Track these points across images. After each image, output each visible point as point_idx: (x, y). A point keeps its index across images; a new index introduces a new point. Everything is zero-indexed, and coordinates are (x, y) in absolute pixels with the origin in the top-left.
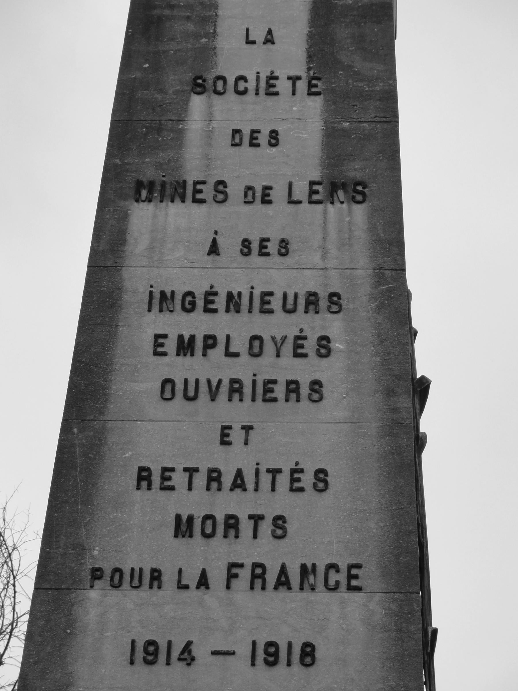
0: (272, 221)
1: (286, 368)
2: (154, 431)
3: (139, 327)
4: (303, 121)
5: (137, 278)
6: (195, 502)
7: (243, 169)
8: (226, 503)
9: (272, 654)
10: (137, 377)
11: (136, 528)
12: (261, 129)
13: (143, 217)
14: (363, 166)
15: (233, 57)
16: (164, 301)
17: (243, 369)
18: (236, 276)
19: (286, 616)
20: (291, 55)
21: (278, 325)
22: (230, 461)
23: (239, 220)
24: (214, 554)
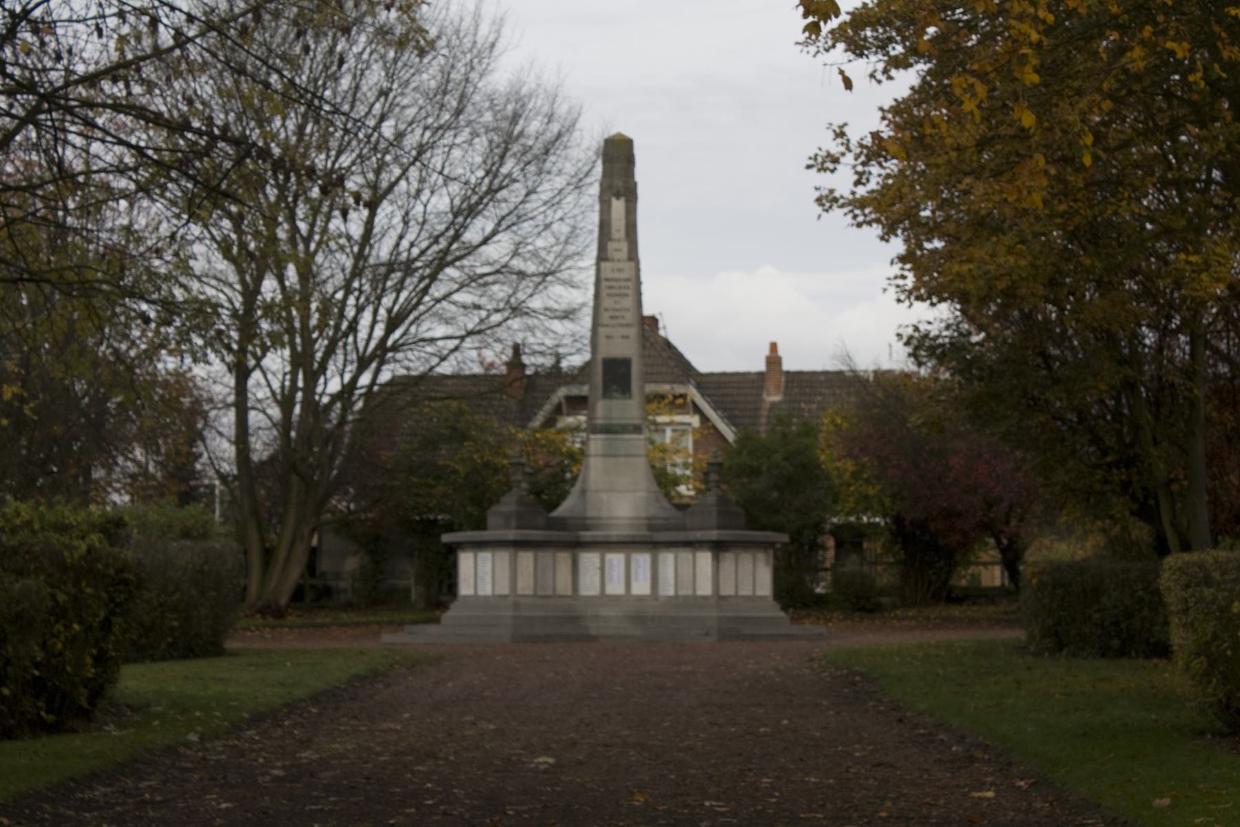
0: (621, 265)
1: (623, 291)
2: (607, 302)
3: (604, 284)
4: (624, 246)
5: (603, 275)
6: (611, 313)
7: (616, 255)
8: (617, 314)
9: (623, 337)
10: (604, 293)
11: (605, 317)
12: (618, 247)
13: (603, 264)
14: (633, 256)
15: (615, 235)
16: (607, 280)
17: (617, 291)
18: (616, 275)
19: (625, 331)
20: (622, 234)
21: (623, 284)
22: (617, 306)
23: (617, 265)
24: (615, 322)
